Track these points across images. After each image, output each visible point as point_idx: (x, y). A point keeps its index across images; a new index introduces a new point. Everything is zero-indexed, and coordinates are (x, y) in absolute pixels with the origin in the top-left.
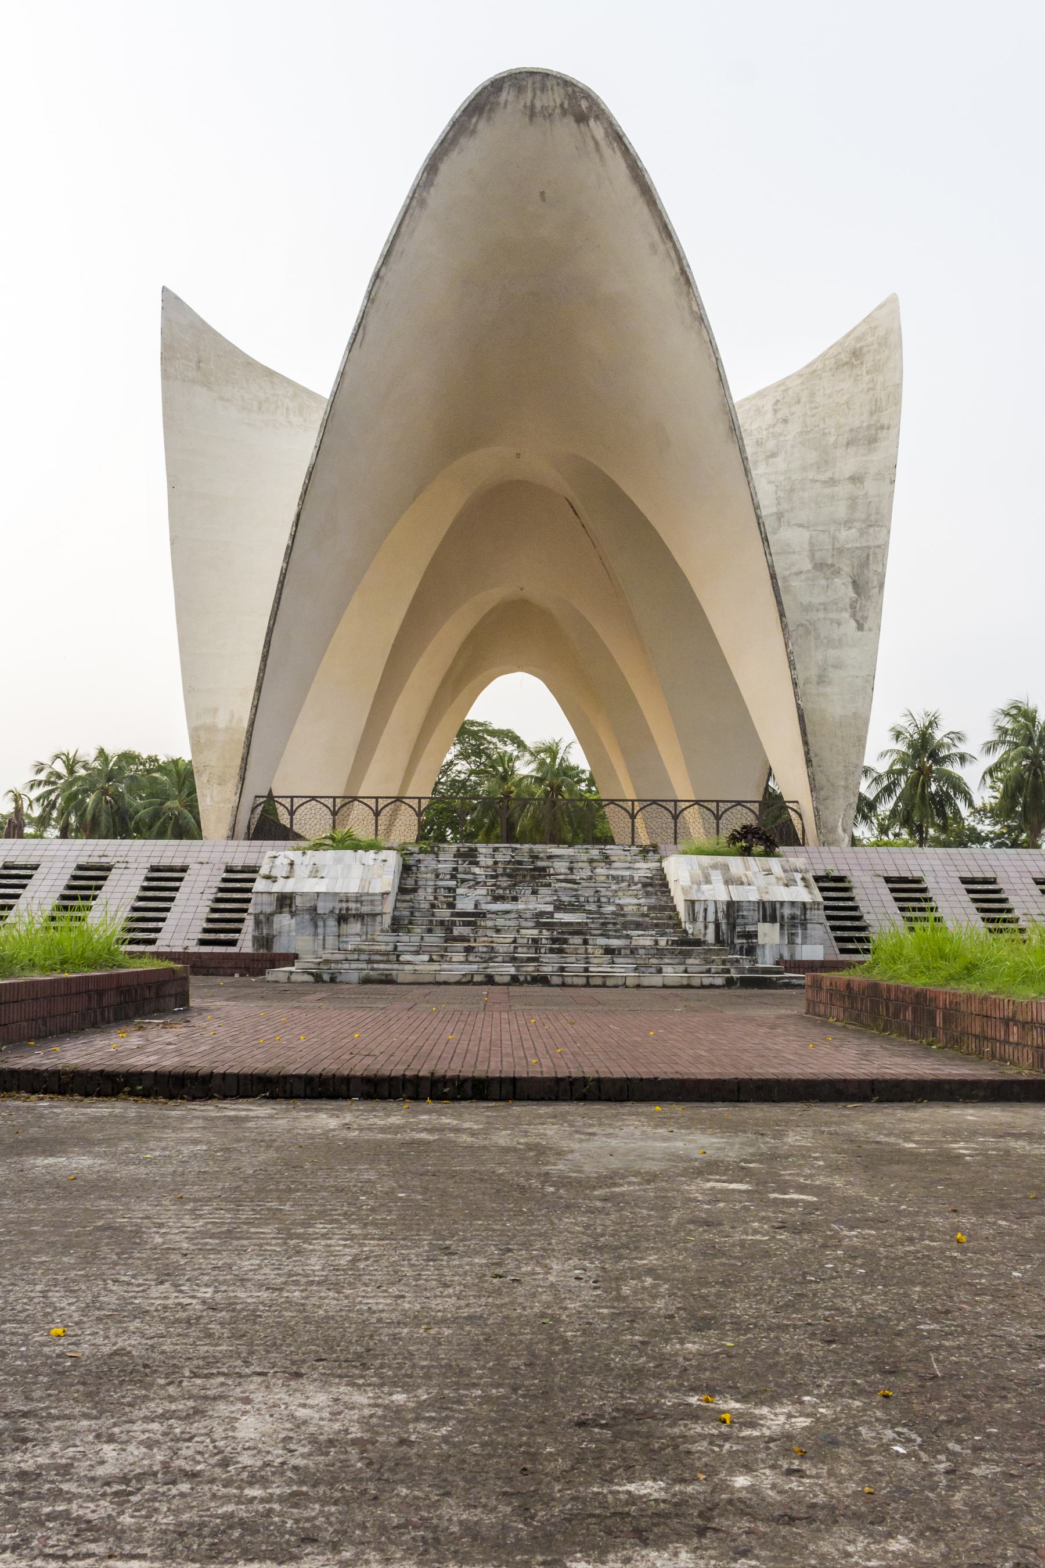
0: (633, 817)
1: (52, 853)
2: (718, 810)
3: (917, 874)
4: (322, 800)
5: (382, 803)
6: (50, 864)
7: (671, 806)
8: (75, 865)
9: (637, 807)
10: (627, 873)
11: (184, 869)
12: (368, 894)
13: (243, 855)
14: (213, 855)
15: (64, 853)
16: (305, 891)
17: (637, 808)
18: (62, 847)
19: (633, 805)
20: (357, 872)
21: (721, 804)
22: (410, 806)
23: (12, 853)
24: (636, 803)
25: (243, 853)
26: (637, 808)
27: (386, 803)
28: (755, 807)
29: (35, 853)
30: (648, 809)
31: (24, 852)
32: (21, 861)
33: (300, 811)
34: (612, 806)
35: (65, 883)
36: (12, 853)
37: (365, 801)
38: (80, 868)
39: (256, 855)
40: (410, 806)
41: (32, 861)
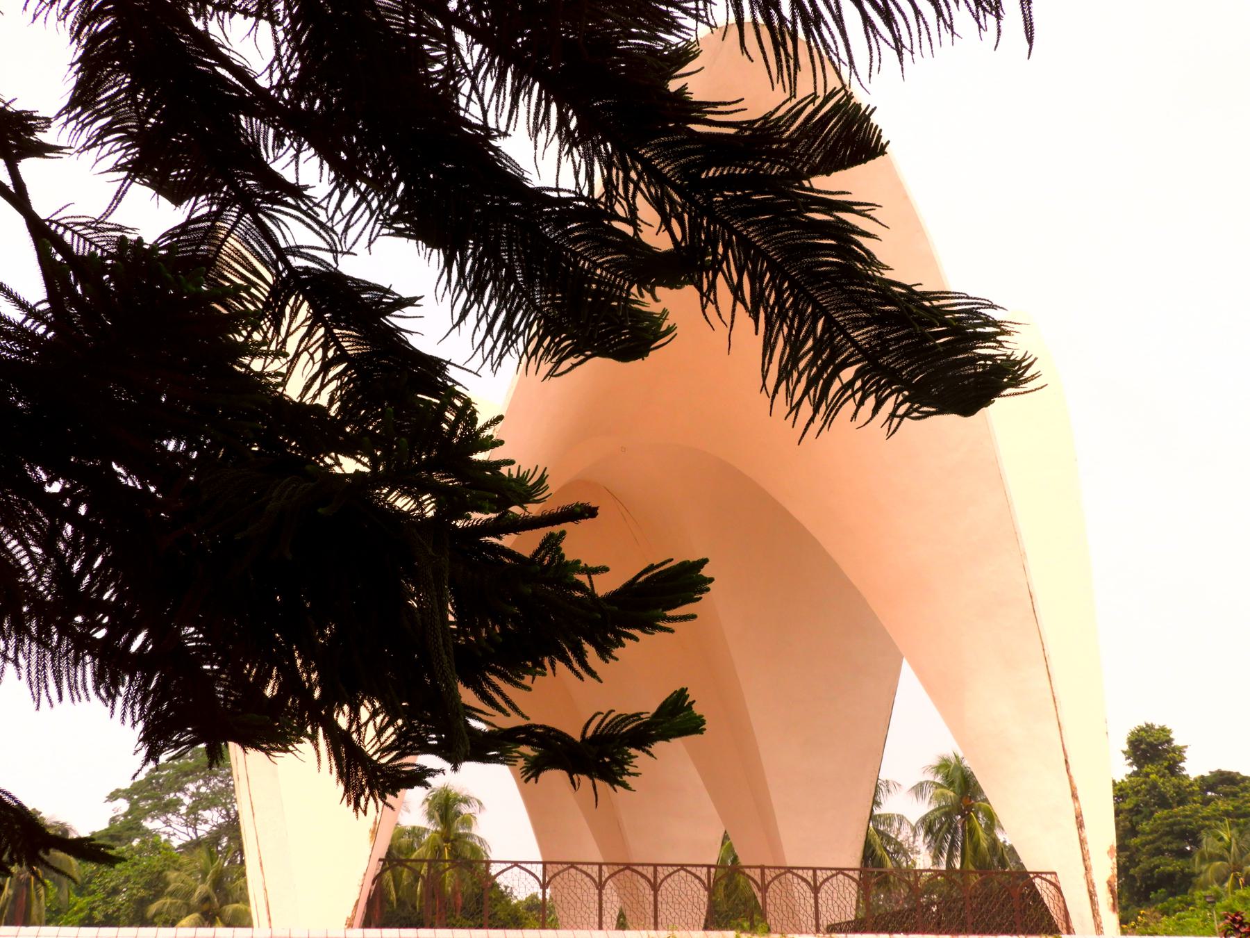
0: (600, 886)
2: (655, 878)
4: (693, 870)
5: (821, 876)
7: (649, 872)
9: (606, 872)
17: (606, 874)
19: (600, 870)
21: (659, 868)
22: (588, 875)
24: (604, 867)
26: (606, 874)
27: (667, 873)
28: (856, 875)
30: (620, 876)
33: (825, 887)
37: (528, 867)
40: (588, 875)
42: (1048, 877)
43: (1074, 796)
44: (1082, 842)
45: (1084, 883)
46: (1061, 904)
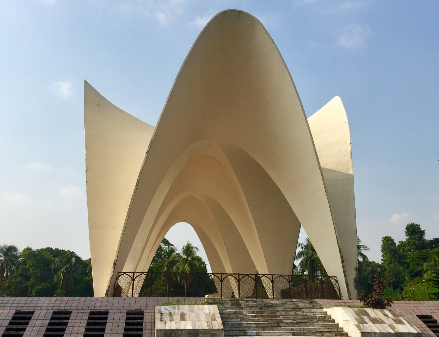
1: (40, 305)
3: (429, 314)
6: (39, 311)
10: (311, 314)
11: (106, 313)
12: (213, 330)
13: (133, 305)
14: (119, 305)
15: (46, 305)
16: (182, 328)
18: (45, 302)
20: (203, 317)
23: (20, 305)
29: (31, 305)
31: (26, 305)
32: (25, 309)
34: (264, 277)
35: (48, 321)
36: (20, 305)
38: (55, 313)
39: (139, 305)
41: (31, 309)
42: (334, 277)
43: (340, 252)
44: (343, 267)
45: (344, 279)
46: (338, 286)
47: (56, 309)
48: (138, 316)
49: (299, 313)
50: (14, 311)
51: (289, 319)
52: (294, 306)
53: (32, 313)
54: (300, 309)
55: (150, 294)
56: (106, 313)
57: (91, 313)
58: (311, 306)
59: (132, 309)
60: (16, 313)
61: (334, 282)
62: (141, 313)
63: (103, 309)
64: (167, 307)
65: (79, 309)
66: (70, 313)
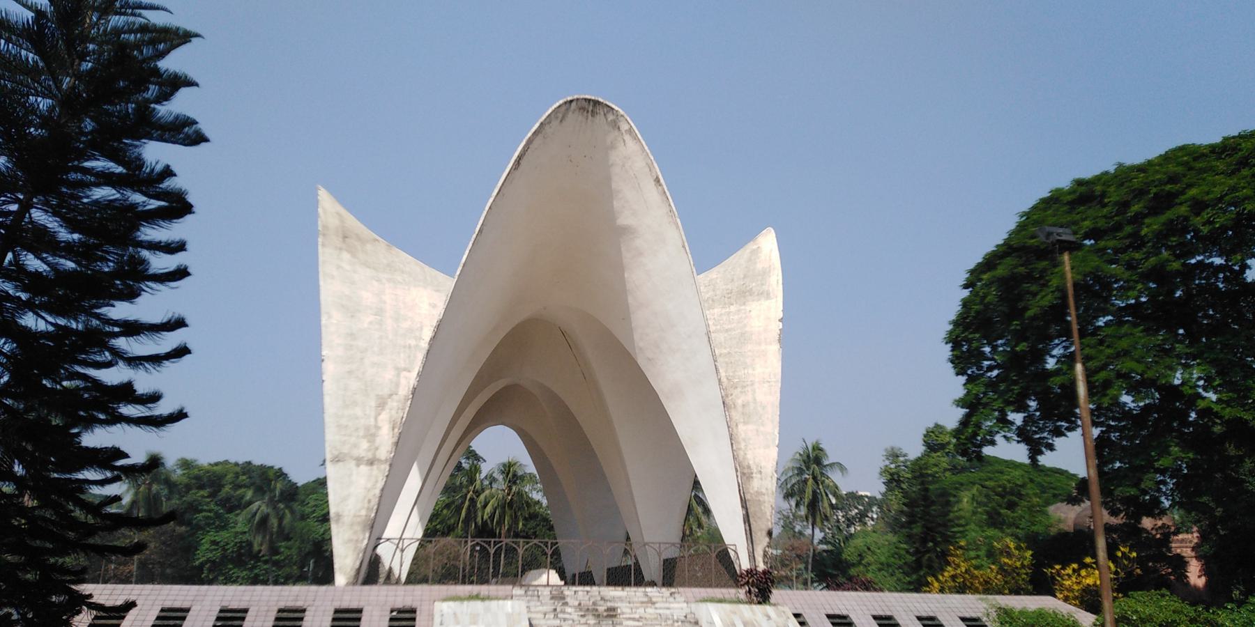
3: (844, 613)
8: (276, 609)
10: (668, 612)
11: (360, 611)
25: (403, 596)
32: (234, 605)
38: (280, 611)
41: (242, 606)
47: (282, 605)
48: (407, 615)
49: (650, 610)
50: (218, 609)
51: (634, 619)
52: (645, 599)
53: (246, 611)
54: (654, 603)
55: (424, 580)
56: (360, 611)
57: (337, 611)
58: (671, 599)
59: (399, 605)
60: (221, 611)
61: (732, 554)
62: (413, 611)
63: (354, 605)
64: (451, 604)
65: (318, 603)
66: (304, 611)
